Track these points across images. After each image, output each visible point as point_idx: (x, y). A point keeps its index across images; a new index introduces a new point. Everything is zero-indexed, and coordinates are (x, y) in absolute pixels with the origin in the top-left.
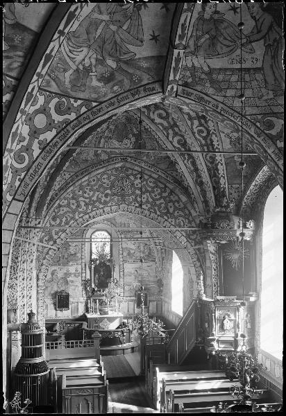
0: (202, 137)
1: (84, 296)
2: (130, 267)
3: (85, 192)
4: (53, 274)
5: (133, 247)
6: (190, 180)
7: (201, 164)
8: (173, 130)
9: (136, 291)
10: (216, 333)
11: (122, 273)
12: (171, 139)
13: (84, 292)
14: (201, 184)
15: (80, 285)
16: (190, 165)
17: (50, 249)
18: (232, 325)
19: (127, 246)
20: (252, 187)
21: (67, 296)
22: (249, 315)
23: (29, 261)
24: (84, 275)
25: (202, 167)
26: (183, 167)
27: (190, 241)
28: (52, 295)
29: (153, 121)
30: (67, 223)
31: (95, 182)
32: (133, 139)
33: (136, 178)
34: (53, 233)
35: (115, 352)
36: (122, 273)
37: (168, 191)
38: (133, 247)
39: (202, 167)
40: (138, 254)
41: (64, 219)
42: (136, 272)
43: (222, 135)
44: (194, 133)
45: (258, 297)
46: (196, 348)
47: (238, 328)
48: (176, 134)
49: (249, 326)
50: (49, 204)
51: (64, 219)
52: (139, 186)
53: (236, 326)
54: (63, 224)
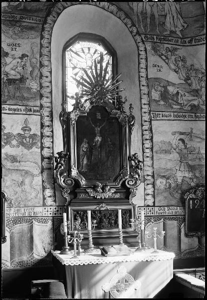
1: (50, 201)
5: (173, 77)
9: (183, 193)
11: (148, 144)
13: (49, 192)
15: (37, 171)
19: (159, 75)
24: (47, 142)
36: (148, 144)
38: (173, 77)
40: (186, 99)
42: (181, 146)
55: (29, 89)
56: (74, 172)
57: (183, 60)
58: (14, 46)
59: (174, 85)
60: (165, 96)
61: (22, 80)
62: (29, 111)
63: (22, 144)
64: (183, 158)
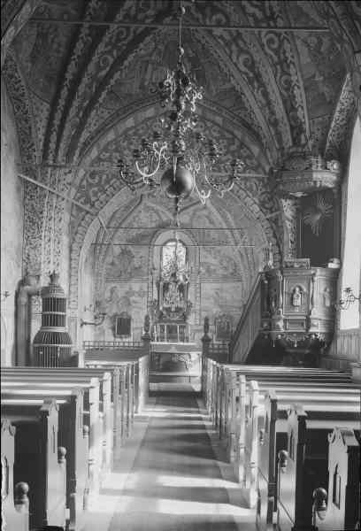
0: (273, 50)
2: (209, 288)
3: (131, 144)
4: (112, 292)
6: (260, 119)
7: (273, 92)
8: (237, 45)
9: (216, 319)
10: (283, 313)
14: (275, 124)
15: (145, 307)
16: (261, 98)
17: (88, 212)
18: (305, 300)
19: (207, 260)
20: (337, 114)
21: (129, 321)
22: (328, 290)
23: (57, 220)
25: (275, 96)
26: (252, 100)
27: (264, 210)
28: (111, 318)
30: (108, 182)
34: (91, 194)
35: (175, 379)
36: (198, 295)
37: (237, 143)
38: (214, 261)
39: (275, 96)
40: (221, 272)
41: (104, 177)
42: (215, 295)
43: (298, 42)
44: (262, 46)
45: (341, 264)
46: (260, 337)
47: (312, 304)
48: (241, 51)
49: (328, 304)
50: (82, 149)
51: (104, 177)
53: (310, 300)
54: (103, 183)
55: (143, 272)
56: (161, 308)
57: (219, 251)
58: (138, 252)
59: (213, 265)
60: (208, 271)
61: (140, 267)
62: (143, 281)
63: (139, 295)
64: (216, 301)
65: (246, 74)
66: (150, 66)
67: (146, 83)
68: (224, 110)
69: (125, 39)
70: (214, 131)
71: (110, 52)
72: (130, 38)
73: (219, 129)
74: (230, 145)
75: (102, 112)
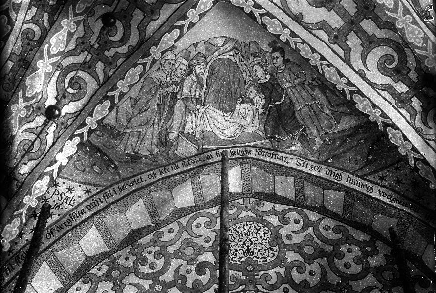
3: (144, 261)
8: (360, 32)
12: (358, 65)
29: (298, 18)
31: (173, 235)
32: (260, 99)
33: (285, 221)
48: (370, 43)
52: (297, 239)
65: (389, 88)
66: (179, 104)
67: (172, 136)
68: (345, 175)
69: (123, 41)
70: (326, 228)
71: (87, 66)
72: (134, 40)
73: (336, 223)
74: (366, 255)
75: (70, 190)
